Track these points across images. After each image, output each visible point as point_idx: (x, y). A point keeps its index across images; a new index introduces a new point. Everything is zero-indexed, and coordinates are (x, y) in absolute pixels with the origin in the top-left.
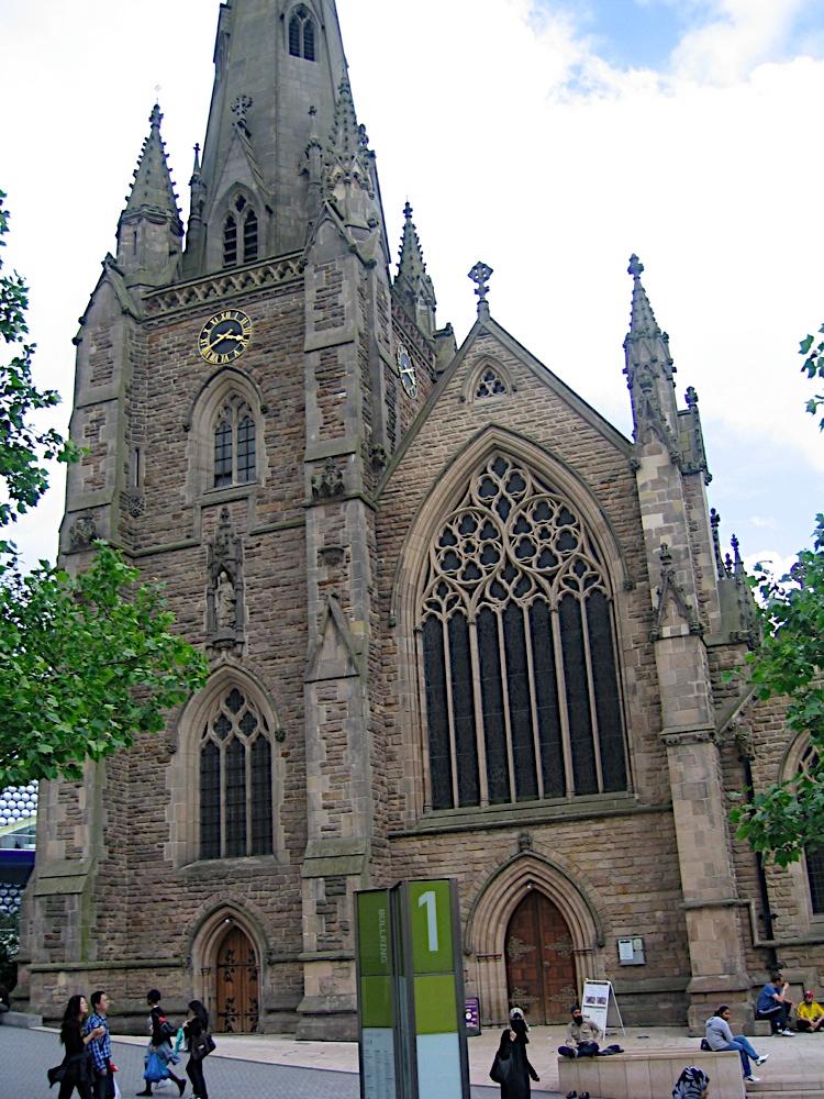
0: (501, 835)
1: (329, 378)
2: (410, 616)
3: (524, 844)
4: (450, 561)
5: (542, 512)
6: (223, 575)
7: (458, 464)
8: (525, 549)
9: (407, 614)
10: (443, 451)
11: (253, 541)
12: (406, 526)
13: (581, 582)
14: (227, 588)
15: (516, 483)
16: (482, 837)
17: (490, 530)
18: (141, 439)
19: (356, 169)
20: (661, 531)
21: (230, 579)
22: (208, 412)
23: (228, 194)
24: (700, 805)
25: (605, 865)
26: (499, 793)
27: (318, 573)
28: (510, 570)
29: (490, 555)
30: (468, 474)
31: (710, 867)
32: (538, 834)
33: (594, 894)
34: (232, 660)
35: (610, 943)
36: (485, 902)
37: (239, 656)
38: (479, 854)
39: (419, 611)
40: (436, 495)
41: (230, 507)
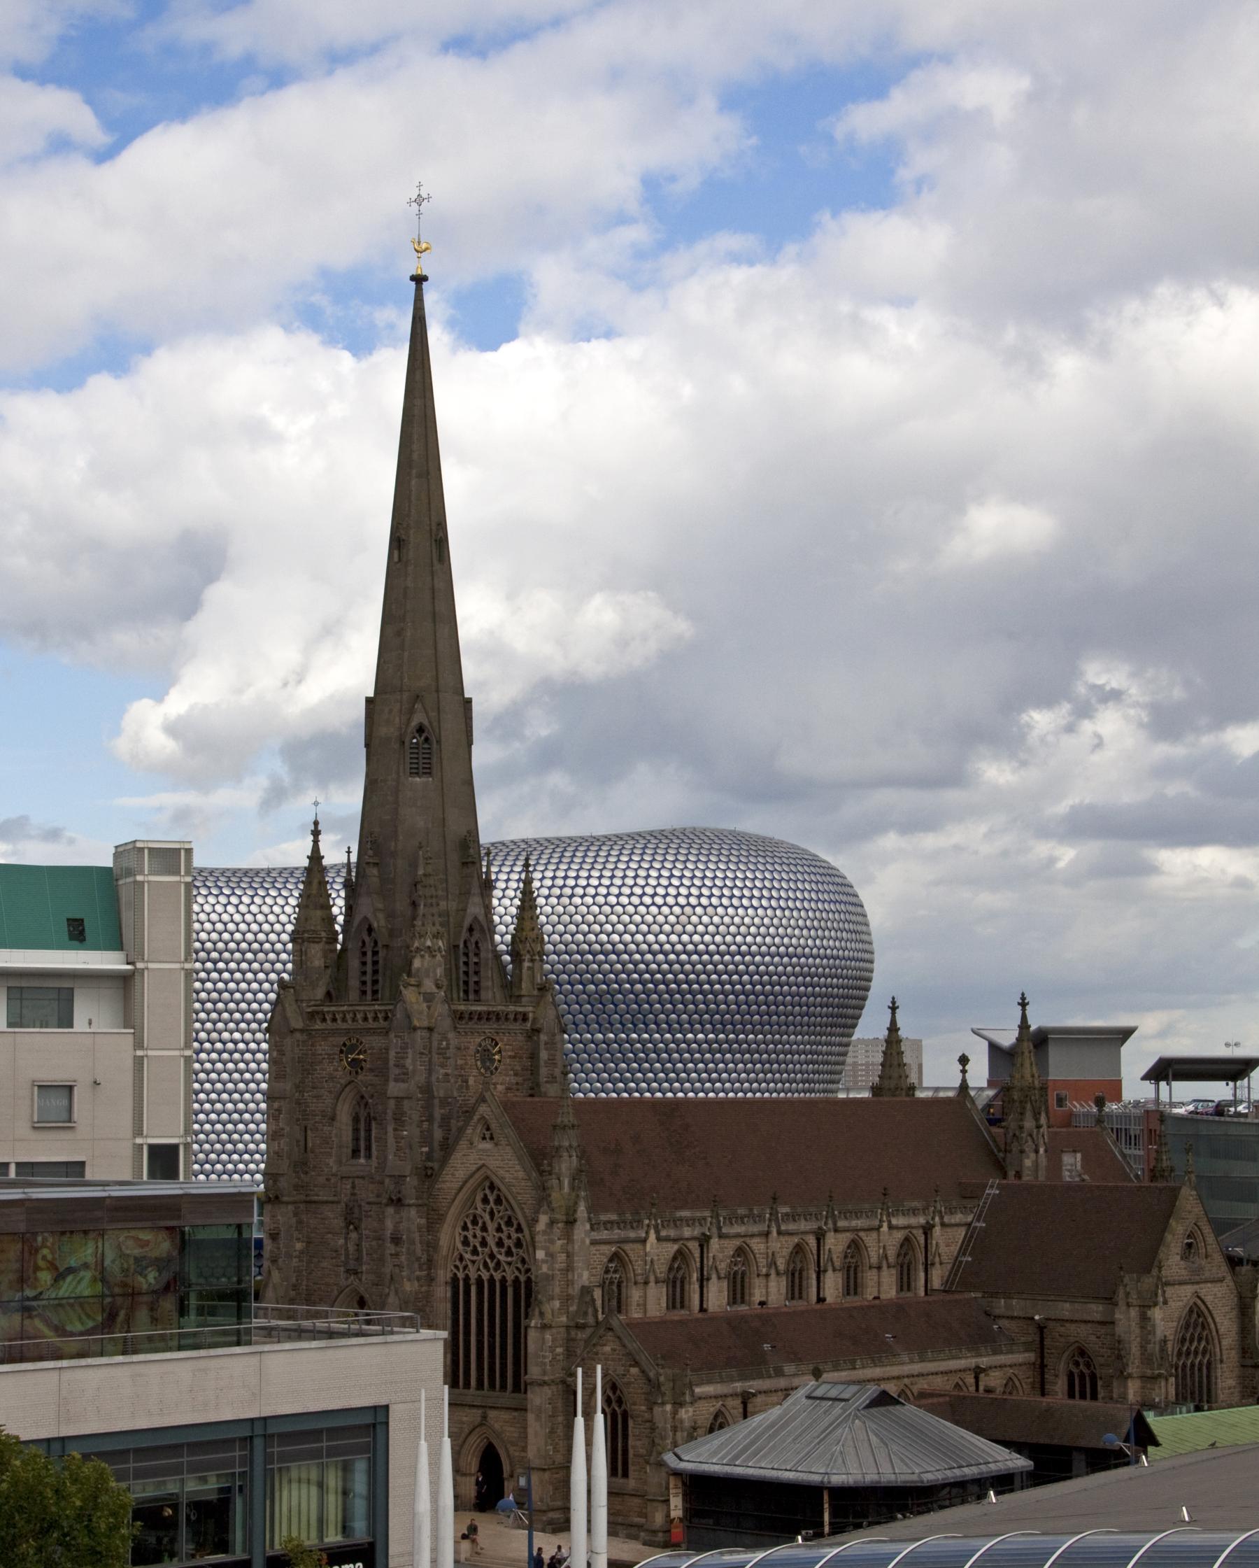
0: (474, 1411)
1: (399, 1120)
2: (443, 1275)
3: (484, 1417)
4: (466, 1242)
5: (509, 1223)
6: (351, 1227)
7: (468, 1185)
8: (500, 1244)
9: (441, 1272)
10: (461, 1174)
11: (367, 1207)
12: (441, 1218)
13: (523, 1270)
14: (354, 1235)
15: (498, 1201)
16: (467, 1409)
17: (484, 1229)
18: (308, 1119)
19: (429, 943)
20: (543, 1261)
21: (356, 1228)
22: (346, 1107)
23: (360, 924)
24: (538, 1418)
25: (516, 1435)
26: (480, 1385)
27: (390, 1248)
28: (492, 1256)
29: (484, 1243)
30: (474, 1192)
31: (539, 1450)
32: (492, 1414)
33: (511, 1449)
34: (356, 1283)
35: (515, 1475)
36: (466, 1446)
37: (360, 1280)
38: (465, 1419)
39: (449, 1270)
40: (456, 1202)
41: (357, 1181)
